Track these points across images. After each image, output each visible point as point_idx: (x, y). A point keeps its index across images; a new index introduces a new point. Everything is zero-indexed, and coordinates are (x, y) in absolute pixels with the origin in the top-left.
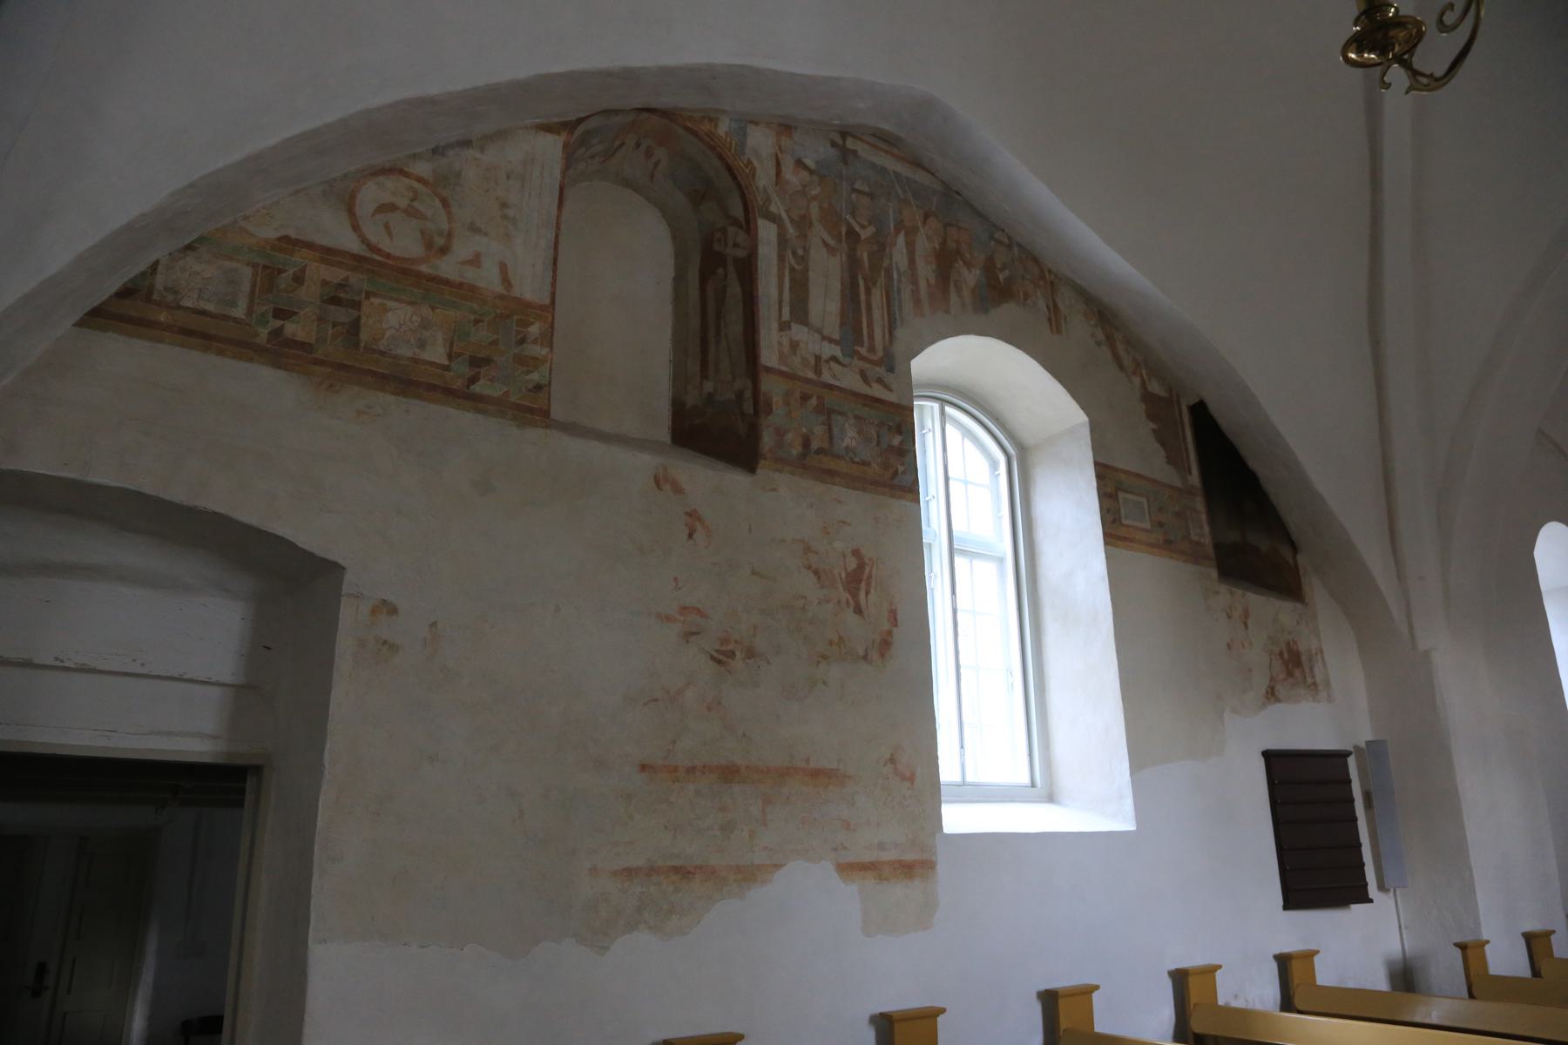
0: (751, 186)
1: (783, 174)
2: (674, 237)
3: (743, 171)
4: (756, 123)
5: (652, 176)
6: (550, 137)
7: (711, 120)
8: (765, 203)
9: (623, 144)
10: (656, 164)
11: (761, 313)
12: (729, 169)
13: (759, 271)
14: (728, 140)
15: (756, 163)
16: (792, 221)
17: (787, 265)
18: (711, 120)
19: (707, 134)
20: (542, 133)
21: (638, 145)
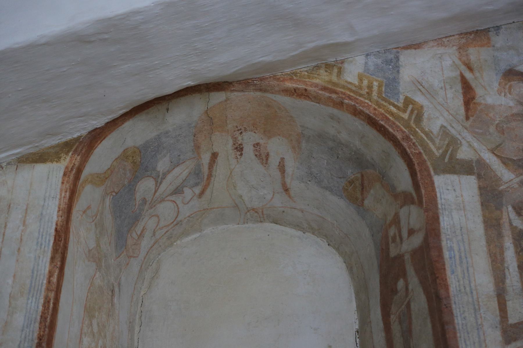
0: (415, 133)
1: (478, 100)
2: (350, 269)
3: (398, 118)
4: (417, 46)
5: (286, 190)
6: (41, 169)
7: (329, 67)
8: (446, 151)
9: (214, 156)
10: (282, 168)
11: (458, 321)
12: (372, 122)
13: (446, 254)
14: (365, 83)
15: (419, 99)
16: (505, 161)
17: (507, 233)
18: (329, 67)
19: (325, 89)
20: (27, 166)
21: (239, 149)
